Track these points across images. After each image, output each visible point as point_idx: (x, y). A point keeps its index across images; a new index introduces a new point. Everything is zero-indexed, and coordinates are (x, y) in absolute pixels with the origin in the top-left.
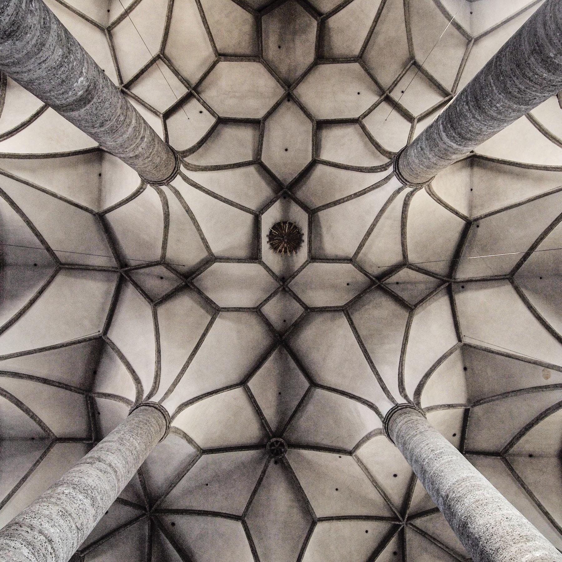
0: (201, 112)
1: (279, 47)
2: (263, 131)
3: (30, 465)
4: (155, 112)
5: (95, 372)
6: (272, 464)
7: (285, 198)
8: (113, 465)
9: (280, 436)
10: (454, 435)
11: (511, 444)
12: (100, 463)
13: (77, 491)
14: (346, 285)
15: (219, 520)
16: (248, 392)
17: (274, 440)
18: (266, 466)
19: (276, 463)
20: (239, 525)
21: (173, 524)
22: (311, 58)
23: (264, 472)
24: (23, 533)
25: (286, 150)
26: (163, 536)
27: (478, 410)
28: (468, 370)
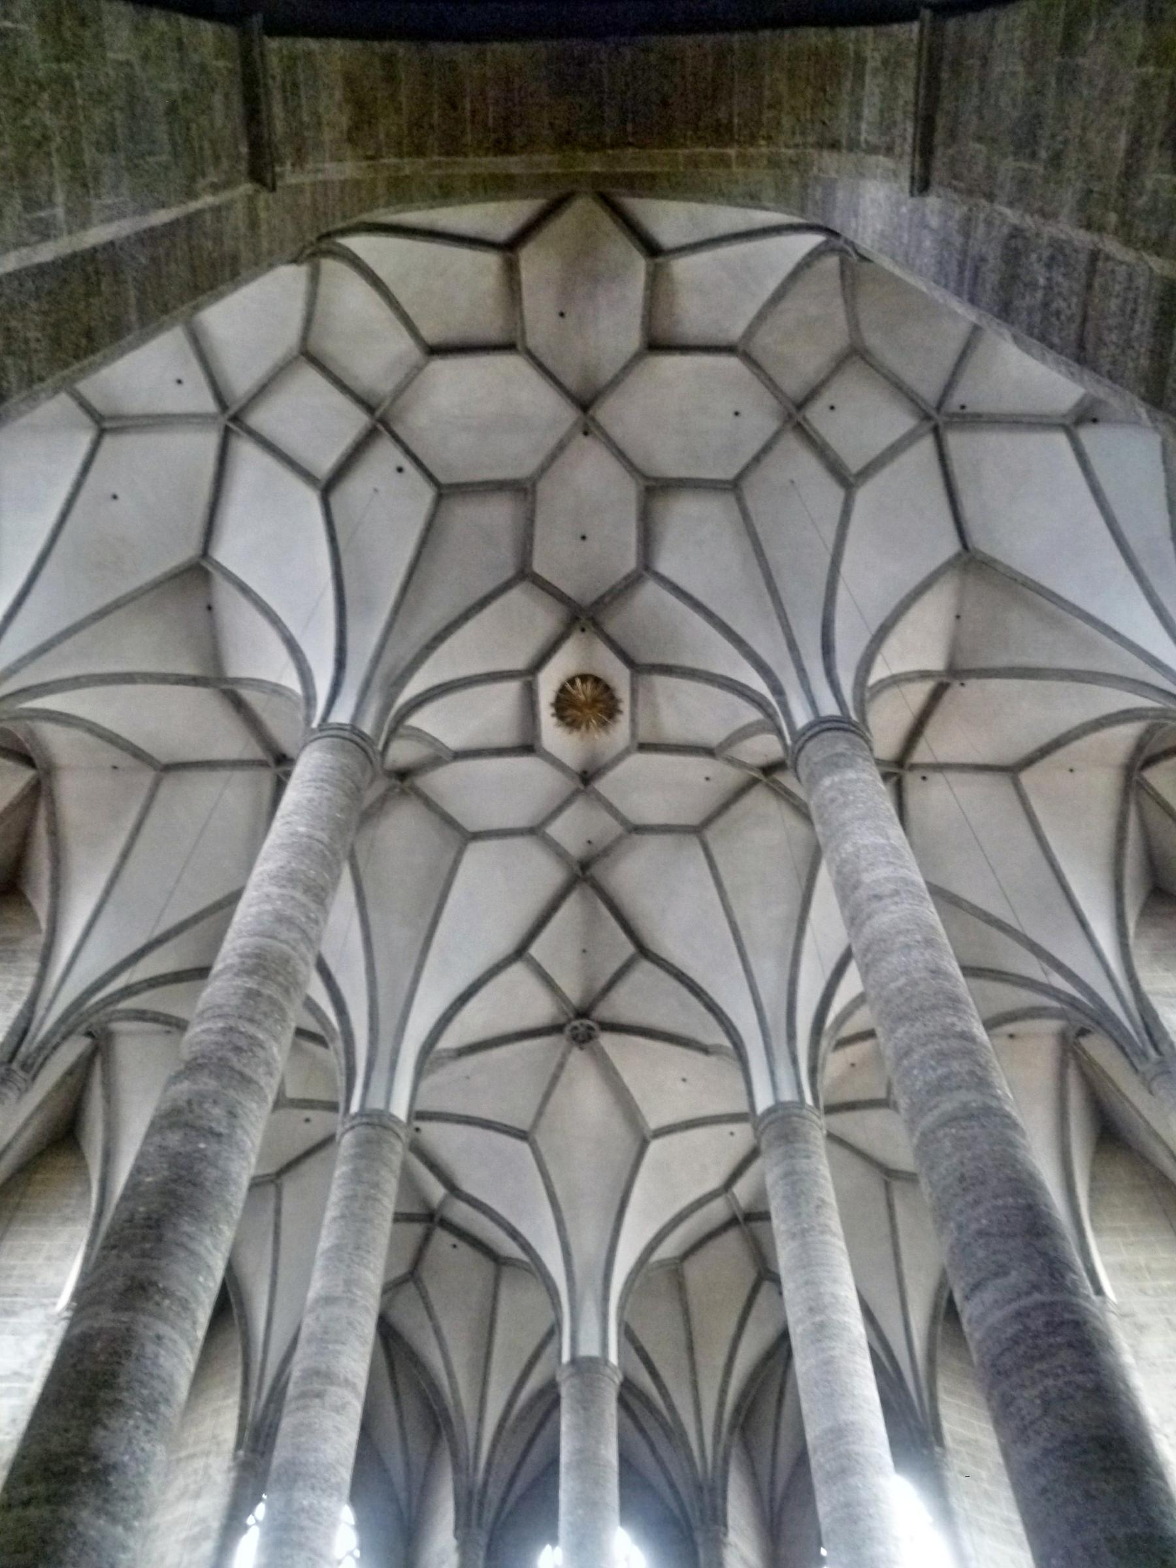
0: (400, 470)
1: (562, 315)
2: (534, 502)
4: (306, 476)
7: (583, 630)
8: (350, 1376)
12: (333, 1389)
13: (319, 1492)
14: (702, 781)
15: (492, 1135)
17: (576, 1023)
19: (582, 1049)
20: (524, 1147)
22: (633, 340)
23: (561, 1066)
25: (584, 538)
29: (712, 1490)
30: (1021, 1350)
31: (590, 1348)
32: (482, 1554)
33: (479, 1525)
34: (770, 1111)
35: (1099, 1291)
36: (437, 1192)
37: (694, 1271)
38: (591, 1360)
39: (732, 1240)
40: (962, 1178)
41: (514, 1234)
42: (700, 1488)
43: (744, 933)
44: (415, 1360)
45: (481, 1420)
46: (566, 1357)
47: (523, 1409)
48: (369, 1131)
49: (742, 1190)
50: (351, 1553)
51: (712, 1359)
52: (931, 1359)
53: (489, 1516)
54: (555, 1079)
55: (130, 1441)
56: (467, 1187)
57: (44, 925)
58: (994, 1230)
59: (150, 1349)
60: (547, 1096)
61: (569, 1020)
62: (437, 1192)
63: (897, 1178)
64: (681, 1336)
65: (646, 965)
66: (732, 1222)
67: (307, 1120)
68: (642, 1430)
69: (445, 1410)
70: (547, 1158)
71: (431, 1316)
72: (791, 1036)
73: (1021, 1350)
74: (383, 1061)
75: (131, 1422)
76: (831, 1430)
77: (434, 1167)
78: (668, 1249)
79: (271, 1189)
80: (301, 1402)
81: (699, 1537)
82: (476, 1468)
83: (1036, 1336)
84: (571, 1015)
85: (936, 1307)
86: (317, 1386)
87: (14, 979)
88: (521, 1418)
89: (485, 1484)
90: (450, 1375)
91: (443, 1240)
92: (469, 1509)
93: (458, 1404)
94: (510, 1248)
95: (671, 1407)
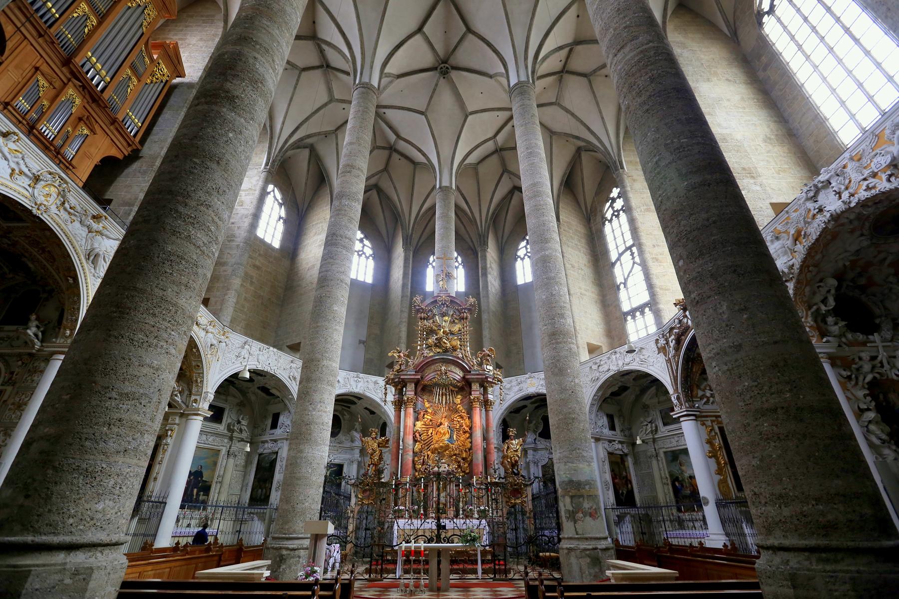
3: (292, 90)
5: (314, 22)
6: (442, 78)
9: (446, 62)
10: (561, 61)
11: (595, 71)
16: (424, 35)
17: (442, 65)
18: (438, 81)
19: (444, 78)
20: (423, 117)
21: (384, 113)
24: (340, 242)
26: (380, 121)
27: (579, 48)
28: (580, 18)
29: (484, 236)
30: (641, 64)
31: (445, 183)
32: (411, 253)
33: (410, 244)
34: (516, 85)
35: (622, 168)
36: (393, 137)
37: (482, 169)
38: (446, 187)
39: (495, 159)
40: (619, 9)
41: (420, 150)
42: (480, 235)
43: (510, 16)
44: (388, 198)
45: (410, 215)
46: (438, 187)
47: (423, 215)
48: (363, 89)
49: (500, 138)
50: (371, 255)
51: (486, 198)
52: (559, 196)
53: (414, 242)
54: (434, 90)
55: (244, 90)
56: (403, 135)
57: (222, 7)
58: (633, 25)
59: (251, 61)
60: (431, 97)
61: (440, 64)
62: (393, 137)
63: (555, 134)
64: (477, 191)
65: (470, 36)
66: (496, 151)
67: (344, 109)
68: (462, 223)
69: (398, 213)
70: (431, 122)
71: (393, 183)
72: (526, 58)
73: (641, 64)
74: (367, 66)
75: (244, 84)
76: (532, 184)
77: (391, 128)
78: (472, 159)
79: (334, 135)
80: (342, 175)
81: (479, 249)
82: (409, 229)
83: (650, 57)
84: (440, 62)
85: (562, 181)
86: (348, 169)
87: (214, 30)
88: (423, 215)
89: (412, 233)
90: (400, 202)
91: (396, 156)
92: (407, 239)
93: (402, 210)
94: (420, 158)
95: (472, 212)
